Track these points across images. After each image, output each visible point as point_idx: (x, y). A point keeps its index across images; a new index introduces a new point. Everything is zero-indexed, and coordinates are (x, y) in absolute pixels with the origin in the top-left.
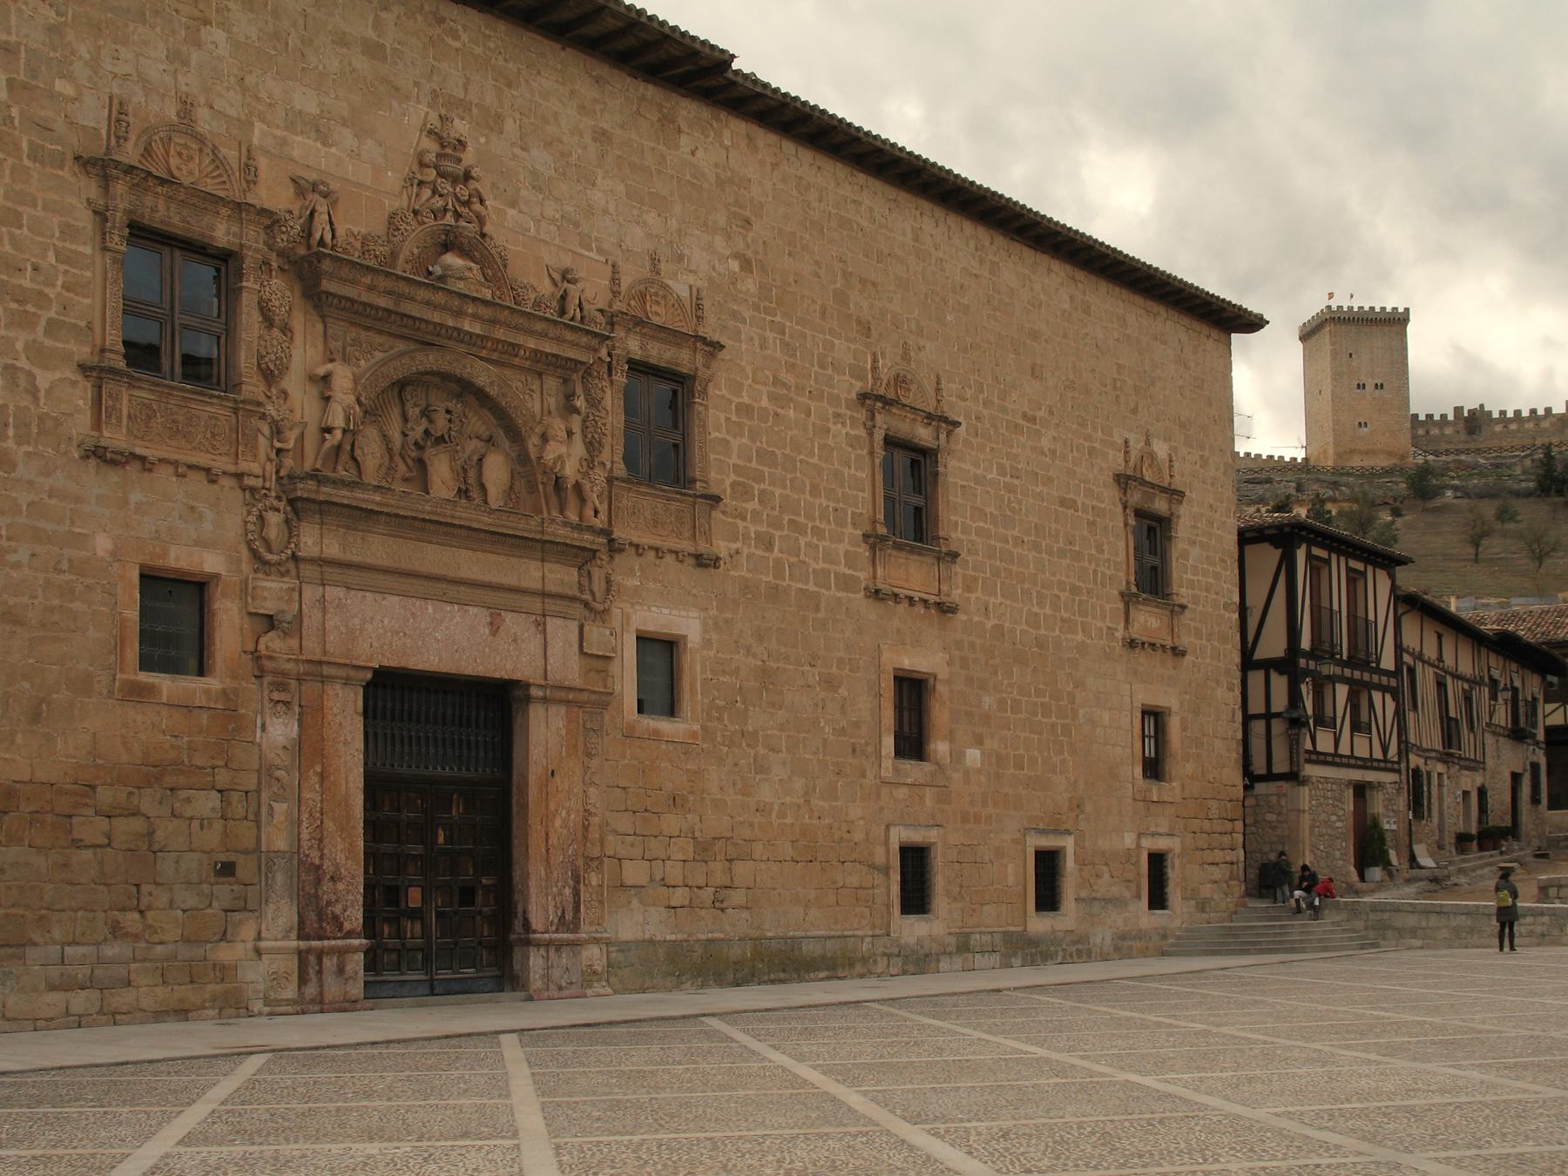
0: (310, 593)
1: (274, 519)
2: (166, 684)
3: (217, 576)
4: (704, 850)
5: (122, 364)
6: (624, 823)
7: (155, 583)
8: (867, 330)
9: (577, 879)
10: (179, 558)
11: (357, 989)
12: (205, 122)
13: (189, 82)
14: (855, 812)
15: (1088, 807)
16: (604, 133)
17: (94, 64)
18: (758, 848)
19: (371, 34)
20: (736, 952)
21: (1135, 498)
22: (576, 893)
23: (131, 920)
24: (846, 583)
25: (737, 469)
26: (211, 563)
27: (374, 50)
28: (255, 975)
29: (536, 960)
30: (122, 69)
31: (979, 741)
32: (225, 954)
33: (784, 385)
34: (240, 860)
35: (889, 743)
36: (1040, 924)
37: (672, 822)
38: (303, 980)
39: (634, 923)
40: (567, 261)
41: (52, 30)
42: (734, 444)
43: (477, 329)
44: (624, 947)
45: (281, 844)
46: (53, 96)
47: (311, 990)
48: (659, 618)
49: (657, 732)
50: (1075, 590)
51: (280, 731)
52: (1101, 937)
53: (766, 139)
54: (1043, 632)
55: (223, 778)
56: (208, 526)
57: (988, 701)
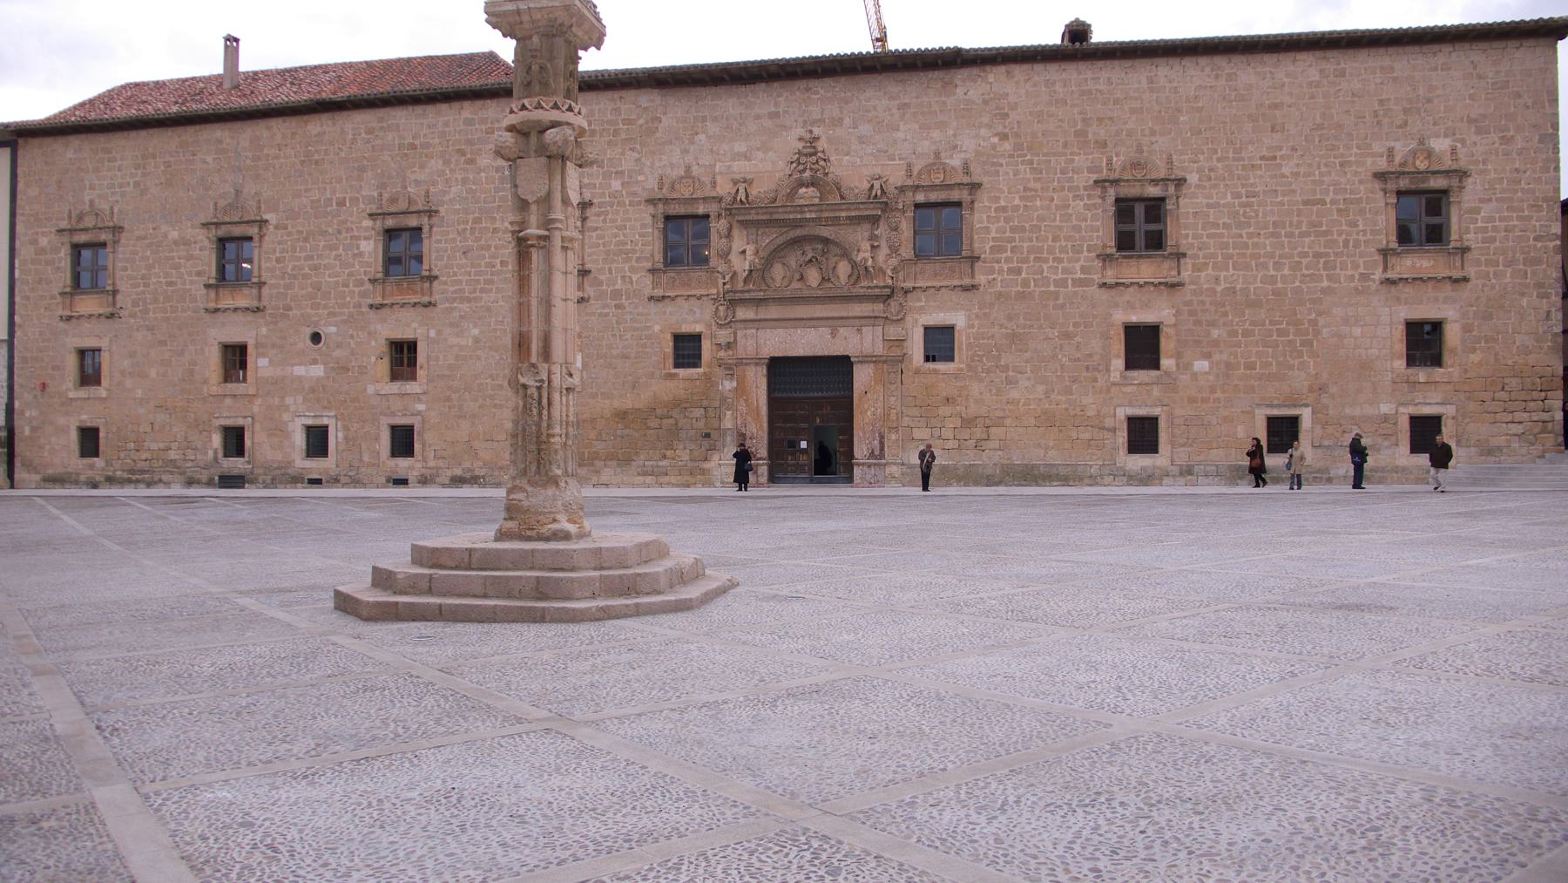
0: (739, 333)
2: (682, 372)
4: (968, 423)
6: (916, 411)
7: (679, 339)
9: (882, 437)
10: (686, 329)
11: (764, 479)
12: (695, 171)
13: (689, 159)
14: (1088, 400)
20: (989, 471)
21: (1391, 186)
23: (669, 453)
26: (698, 328)
29: (857, 471)
31: (1207, 356)
32: (706, 465)
37: (945, 410)
40: (878, 171)
41: (638, 160)
42: (993, 228)
45: (729, 425)
48: (937, 318)
49: (936, 371)
50: (1317, 255)
55: (705, 403)
57: (1215, 333)
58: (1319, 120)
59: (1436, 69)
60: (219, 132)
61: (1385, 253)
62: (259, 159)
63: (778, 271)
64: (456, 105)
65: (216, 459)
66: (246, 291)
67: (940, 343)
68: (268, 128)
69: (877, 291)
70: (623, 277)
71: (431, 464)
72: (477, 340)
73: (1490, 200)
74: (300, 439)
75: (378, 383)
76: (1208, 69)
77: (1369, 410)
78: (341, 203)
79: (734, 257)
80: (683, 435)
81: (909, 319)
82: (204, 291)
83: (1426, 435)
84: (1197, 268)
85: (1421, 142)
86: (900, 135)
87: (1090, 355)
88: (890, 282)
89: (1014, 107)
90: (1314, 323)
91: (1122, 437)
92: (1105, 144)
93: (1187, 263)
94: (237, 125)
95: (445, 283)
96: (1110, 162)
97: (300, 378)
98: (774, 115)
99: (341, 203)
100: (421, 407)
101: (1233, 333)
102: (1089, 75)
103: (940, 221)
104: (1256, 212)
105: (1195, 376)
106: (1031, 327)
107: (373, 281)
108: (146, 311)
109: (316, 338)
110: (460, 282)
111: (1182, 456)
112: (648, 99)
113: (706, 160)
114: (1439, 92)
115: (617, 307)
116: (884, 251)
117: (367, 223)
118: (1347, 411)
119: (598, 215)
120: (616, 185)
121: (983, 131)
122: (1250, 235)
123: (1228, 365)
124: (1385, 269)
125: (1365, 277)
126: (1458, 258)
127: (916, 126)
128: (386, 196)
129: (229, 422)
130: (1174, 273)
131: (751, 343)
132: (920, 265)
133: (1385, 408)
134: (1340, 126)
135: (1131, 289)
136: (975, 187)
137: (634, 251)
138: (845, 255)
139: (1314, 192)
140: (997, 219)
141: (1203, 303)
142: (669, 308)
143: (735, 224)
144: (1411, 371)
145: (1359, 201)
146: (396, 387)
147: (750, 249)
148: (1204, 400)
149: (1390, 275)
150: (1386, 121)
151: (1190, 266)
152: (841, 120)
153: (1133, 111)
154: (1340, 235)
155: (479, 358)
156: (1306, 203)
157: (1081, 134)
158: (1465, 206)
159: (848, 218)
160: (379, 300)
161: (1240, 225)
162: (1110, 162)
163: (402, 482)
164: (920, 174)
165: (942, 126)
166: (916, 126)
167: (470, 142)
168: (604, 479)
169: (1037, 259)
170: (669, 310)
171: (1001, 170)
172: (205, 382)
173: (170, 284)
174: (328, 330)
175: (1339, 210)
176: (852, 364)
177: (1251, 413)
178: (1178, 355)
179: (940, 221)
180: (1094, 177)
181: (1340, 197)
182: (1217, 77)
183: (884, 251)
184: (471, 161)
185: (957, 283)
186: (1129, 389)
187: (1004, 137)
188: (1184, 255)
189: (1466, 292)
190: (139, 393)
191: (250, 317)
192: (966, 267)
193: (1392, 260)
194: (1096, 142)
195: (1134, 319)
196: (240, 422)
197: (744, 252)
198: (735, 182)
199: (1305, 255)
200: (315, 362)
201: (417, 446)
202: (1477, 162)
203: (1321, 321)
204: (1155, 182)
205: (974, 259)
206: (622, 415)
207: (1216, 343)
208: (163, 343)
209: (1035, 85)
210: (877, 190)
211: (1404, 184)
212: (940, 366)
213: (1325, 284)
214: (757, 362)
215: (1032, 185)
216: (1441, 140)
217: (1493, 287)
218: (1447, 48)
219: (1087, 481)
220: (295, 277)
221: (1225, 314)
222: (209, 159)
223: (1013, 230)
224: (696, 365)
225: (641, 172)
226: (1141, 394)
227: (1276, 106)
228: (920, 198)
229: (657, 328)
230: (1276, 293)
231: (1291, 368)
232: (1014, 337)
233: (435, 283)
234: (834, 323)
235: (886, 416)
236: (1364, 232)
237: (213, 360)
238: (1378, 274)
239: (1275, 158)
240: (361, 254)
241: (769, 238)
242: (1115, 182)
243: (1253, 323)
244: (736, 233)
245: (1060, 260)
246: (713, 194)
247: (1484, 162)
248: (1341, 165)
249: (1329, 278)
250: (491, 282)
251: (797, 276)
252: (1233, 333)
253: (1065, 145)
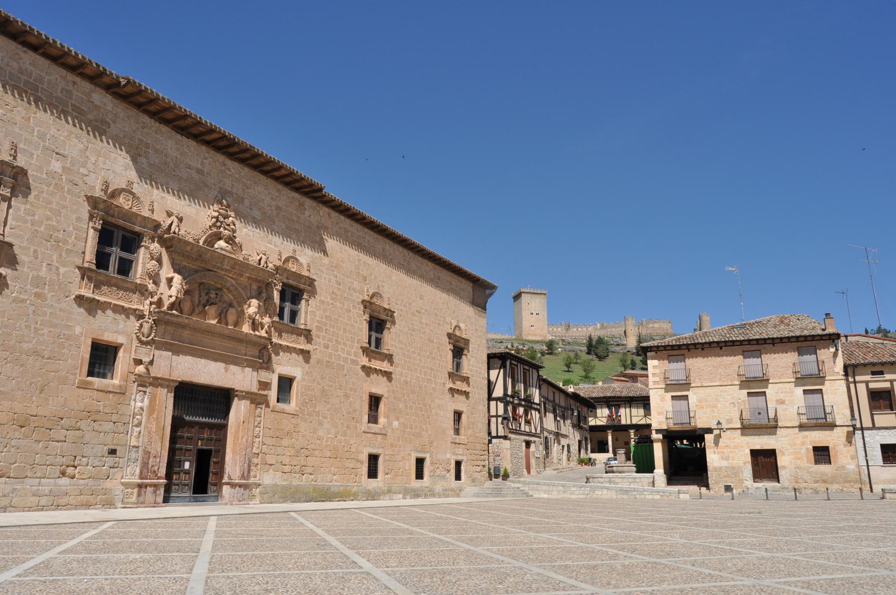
3: (122, 344)
5: (94, 267)
6: (268, 441)
8: (365, 279)
9: (250, 461)
11: (160, 499)
14: (352, 442)
15: (435, 444)
16: (279, 207)
19: (199, 166)
22: (249, 466)
25: (318, 322)
26: (120, 339)
27: (200, 172)
30: (106, 167)
31: (397, 419)
34: (118, 448)
35: (366, 418)
36: (417, 484)
39: (268, 478)
42: (318, 313)
47: (141, 499)
52: (438, 488)
53: (334, 214)
55: (115, 418)
56: (121, 326)
115: (37, 295)
120: (56, 166)
133: (448, 456)
177: (410, 455)
178: (387, 417)
215: (336, 291)
229: (78, 330)
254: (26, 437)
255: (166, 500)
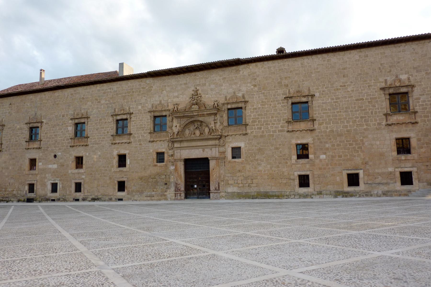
0: (175, 152)
1: (170, 144)
4: (246, 178)
6: (229, 175)
10: (160, 151)
11: (183, 198)
12: (163, 102)
13: (161, 98)
14: (284, 170)
17: (150, 101)
18: (259, 177)
20: (253, 194)
21: (387, 92)
23: (155, 190)
24: (280, 131)
25: (253, 118)
26: (163, 150)
28: (169, 196)
31: (325, 153)
32: (166, 193)
33: (264, 102)
37: (238, 174)
38: (175, 196)
39: (230, 190)
40: (216, 99)
41: (146, 100)
42: (252, 115)
43: (196, 114)
44: (228, 193)
45: (172, 181)
46: (146, 106)
47: (176, 198)
49: (235, 162)
50: (362, 117)
51: (172, 168)
54: (349, 128)
55: (165, 174)
57: (327, 146)
58: (360, 72)
59: (400, 52)
60: (31, 96)
61: (386, 115)
62: (42, 104)
63: (187, 132)
64: (95, 85)
65: (26, 193)
66: (37, 142)
67: (236, 152)
68: (45, 95)
69: (216, 137)
70: (142, 135)
71: (86, 194)
72: (100, 156)
73: (424, 95)
74: (49, 187)
75: (72, 170)
76: (321, 59)
77: (384, 170)
78: (63, 116)
79: (174, 128)
80: (159, 184)
81: (227, 145)
82: (25, 143)
83: (406, 178)
84: (320, 124)
85: (397, 77)
86: (223, 87)
87: (285, 155)
88: (220, 134)
89: (258, 76)
90: (362, 141)
91: (297, 182)
92: (287, 85)
93: (316, 123)
94: (36, 94)
95: (91, 139)
96: (289, 92)
97: (50, 168)
98: (186, 84)
99: (63, 116)
100: (84, 177)
101: (333, 145)
102: (282, 64)
103: (235, 113)
104: (339, 104)
105: (321, 160)
106: (265, 146)
107: (71, 139)
108: (9, 150)
109: (55, 156)
110: (95, 138)
111: (318, 189)
112: (149, 81)
113: (166, 99)
114: (402, 59)
115: (140, 144)
116: (219, 124)
117: (70, 121)
118: (376, 171)
119: (135, 117)
121: (249, 85)
122: (338, 112)
123: (333, 157)
124: (387, 120)
125: (379, 124)
126: (413, 115)
127: (228, 84)
128: (76, 113)
129: (30, 182)
130: (312, 126)
131: (179, 154)
132: (229, 128)
133: (390, 169)
134: (367, 74)
135: (298, 132)
136: (246, 102)
137: (145, 127)
138: (207, 126)
139: (359, 96)
140: (253, 112)
141: (322, 136)
142: (154, 144)
143: (174, 118)
144: (399, 156)
145: (376, 98)
146: (77, 171)
147: (178, 125)
148: (325, 169)
149: (389, 122)
150: (383, 70)
151: (317, 124)
152: (205, 84)
153: (296, 74)
154: (369, 110)
155: (100, 161)
156: (357, 100)
157: (280, 83)
158: (415, 97)
159: (207, 114)
160: (73, 144)
161: (334, 109)
162: (289, 92)
163: (77, 200)
164: (229, 99)
165: (236, 84)
166: (228, 84)
167: (99, 96)
168: (135, 199)
169: (266, 124)
170: (155, 145)
171: (254, 96)
172: (24, 170)
173: (16, 141)
174: (59, 154)
175: (369, 102)
176: (209, 160)
177: (342, 172)
178: (315, 154)
179: (235, 113)
180: (284, 96)
181: (369, 97)
182: (324, 61)
183: (219, 124)
184: (99, 102)
185: (241, 133)
186: (298, 166)
187: (255, 86)
188: (315, 120)
189: (417, 127)
190: (6, 174)
191: (37, 150)
192: (244, 127)
193: (389, 117)
194: (285, 85)
195: (299, 142)
196: (33, 182)
197: (176, 126)
198: (174, 105)
199: (358, 118)
200: (54, 164)
201: (82, 189)
202: (418, 82)
203: (365, 140)
204: (304, 96)
205: (246, 125)
206: (141, 179)
207: (327, 149)
208: (14, 159)
209: (265, 68)
210: (216, 105)
211: (391, 91)
212: (236, 160)
213: (365, 127)
214: (180, 160)
215: (264, 100)
216: (404, 75)
217: (427, 125)
218: (403, 44)
219: (286, 197)
220: (50, 138)
221: (330, 139)
222: (28, 104)
223: (258, 115)
224: (163, 162)
225: (147, 103)
226: (302, 167)
227: (344, 69)
228: (229, 107)
229: (151, 151)
230: (348, 131)
231: (355, 156)
232: (260, 150)
233: (89, 139)
234: (204, 147)
235: (220, 177)
236: (378, 108)
237: (27, 163)
238: (384, 123)
239: (345, 86)
240: (68, 131)
241: (184, 121)
242: (291, 97)
243: (340, 142)
244: (174, 120)
245: (273, 124)
246: (168, 109)
247: (420, 82)
248: (369, 86)
249: (367, 125)
250: (104, 138)
251: (193, 133)
252: (333, 145)
253: (275, 87)
254: (142, 182)
255: (186, 197)
